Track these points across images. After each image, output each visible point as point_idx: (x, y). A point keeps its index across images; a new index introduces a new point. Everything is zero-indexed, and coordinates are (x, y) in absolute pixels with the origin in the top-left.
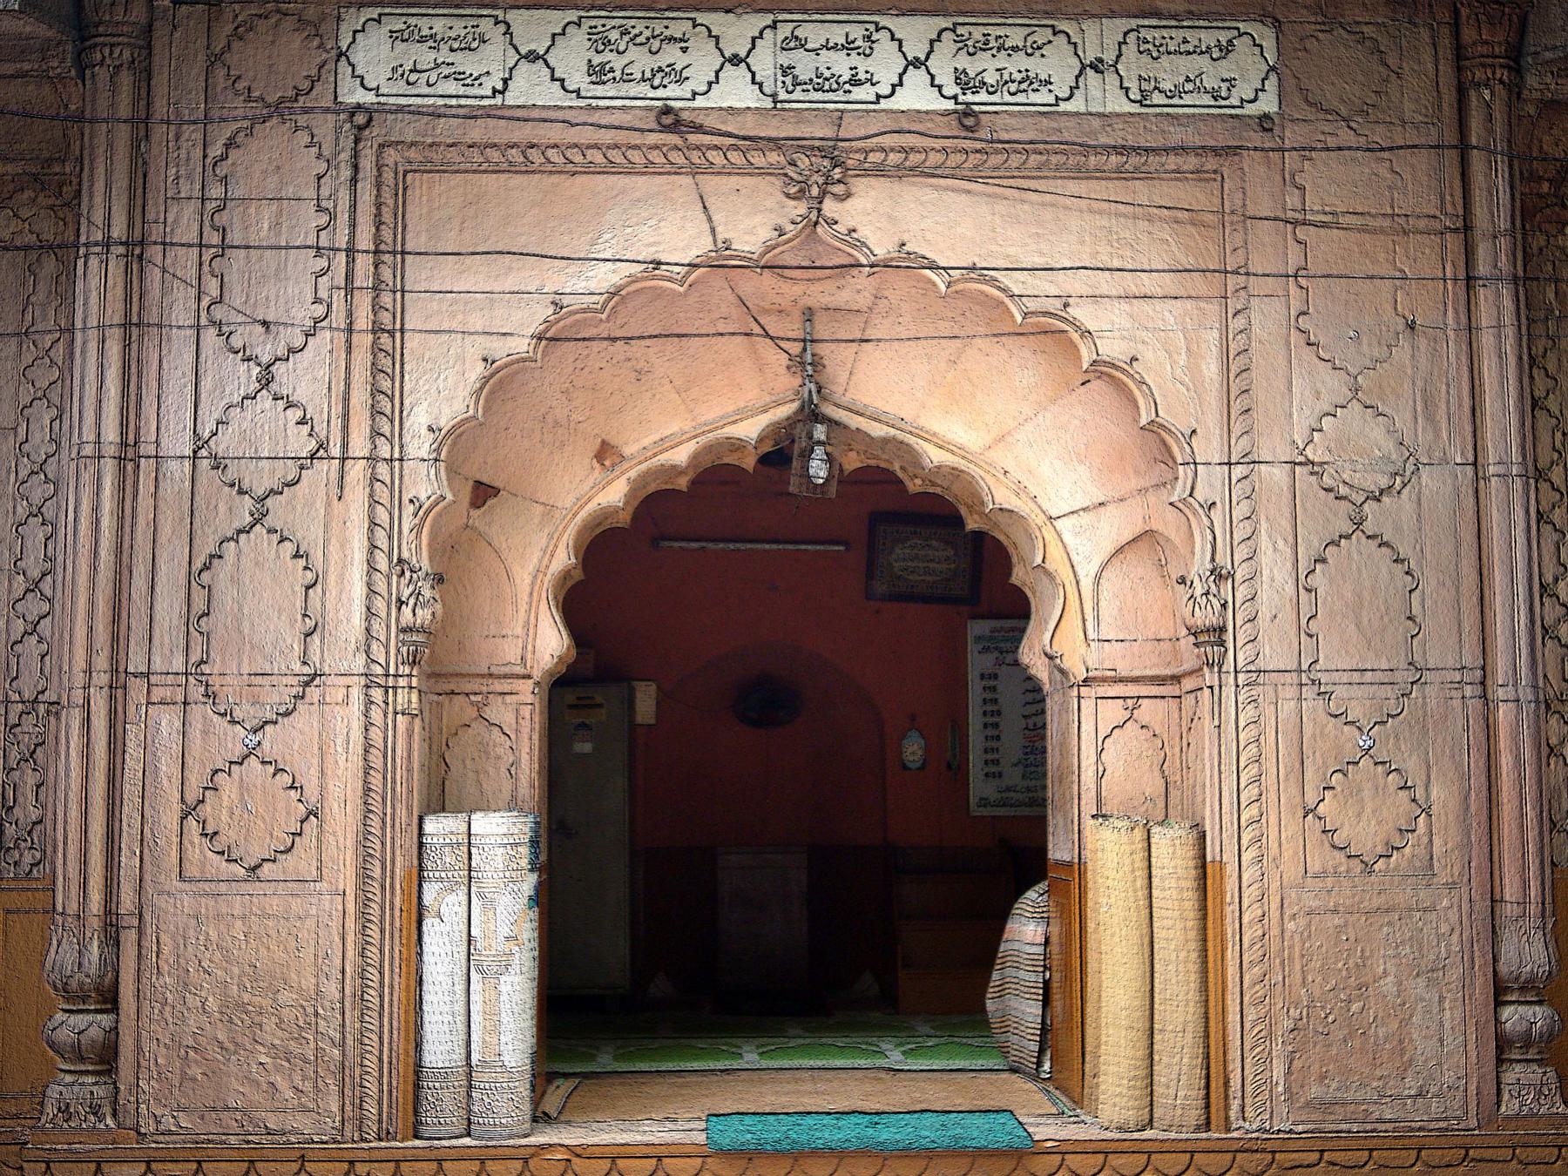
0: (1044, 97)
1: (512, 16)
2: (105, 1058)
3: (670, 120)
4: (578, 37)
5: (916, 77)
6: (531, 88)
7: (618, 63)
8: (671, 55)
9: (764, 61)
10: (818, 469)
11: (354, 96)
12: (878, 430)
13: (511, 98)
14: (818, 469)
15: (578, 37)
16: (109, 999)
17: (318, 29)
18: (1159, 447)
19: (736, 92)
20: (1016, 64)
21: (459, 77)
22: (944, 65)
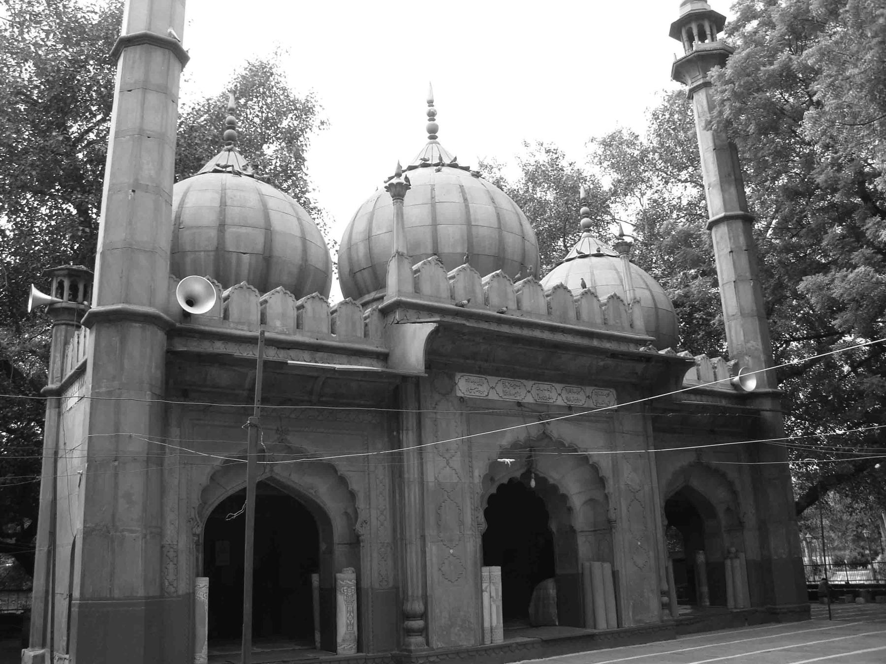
0: (581, 404)
1: (488, 377)
2: (424, 631)
3: (519, 404)
4: (500, 385)
5: (560, 398)
6: (493, 396)
7: (508, 390)
8: (517, 389)
9: (534, 392)
10: (533, 483)
11: (460, 394)
12: (541, 475)
13: (490, 397)
14: (533, 483)
15: (500, 385)
16: (424, 616)
17: (452, 377)
18: (601, 482)
19: (529, 399)
20: (576, 396)
21: (479, 391)
22: (564, 395)
